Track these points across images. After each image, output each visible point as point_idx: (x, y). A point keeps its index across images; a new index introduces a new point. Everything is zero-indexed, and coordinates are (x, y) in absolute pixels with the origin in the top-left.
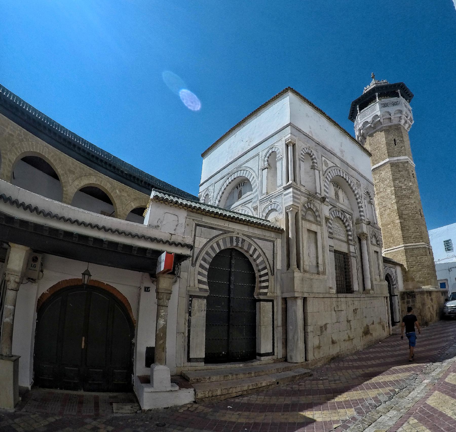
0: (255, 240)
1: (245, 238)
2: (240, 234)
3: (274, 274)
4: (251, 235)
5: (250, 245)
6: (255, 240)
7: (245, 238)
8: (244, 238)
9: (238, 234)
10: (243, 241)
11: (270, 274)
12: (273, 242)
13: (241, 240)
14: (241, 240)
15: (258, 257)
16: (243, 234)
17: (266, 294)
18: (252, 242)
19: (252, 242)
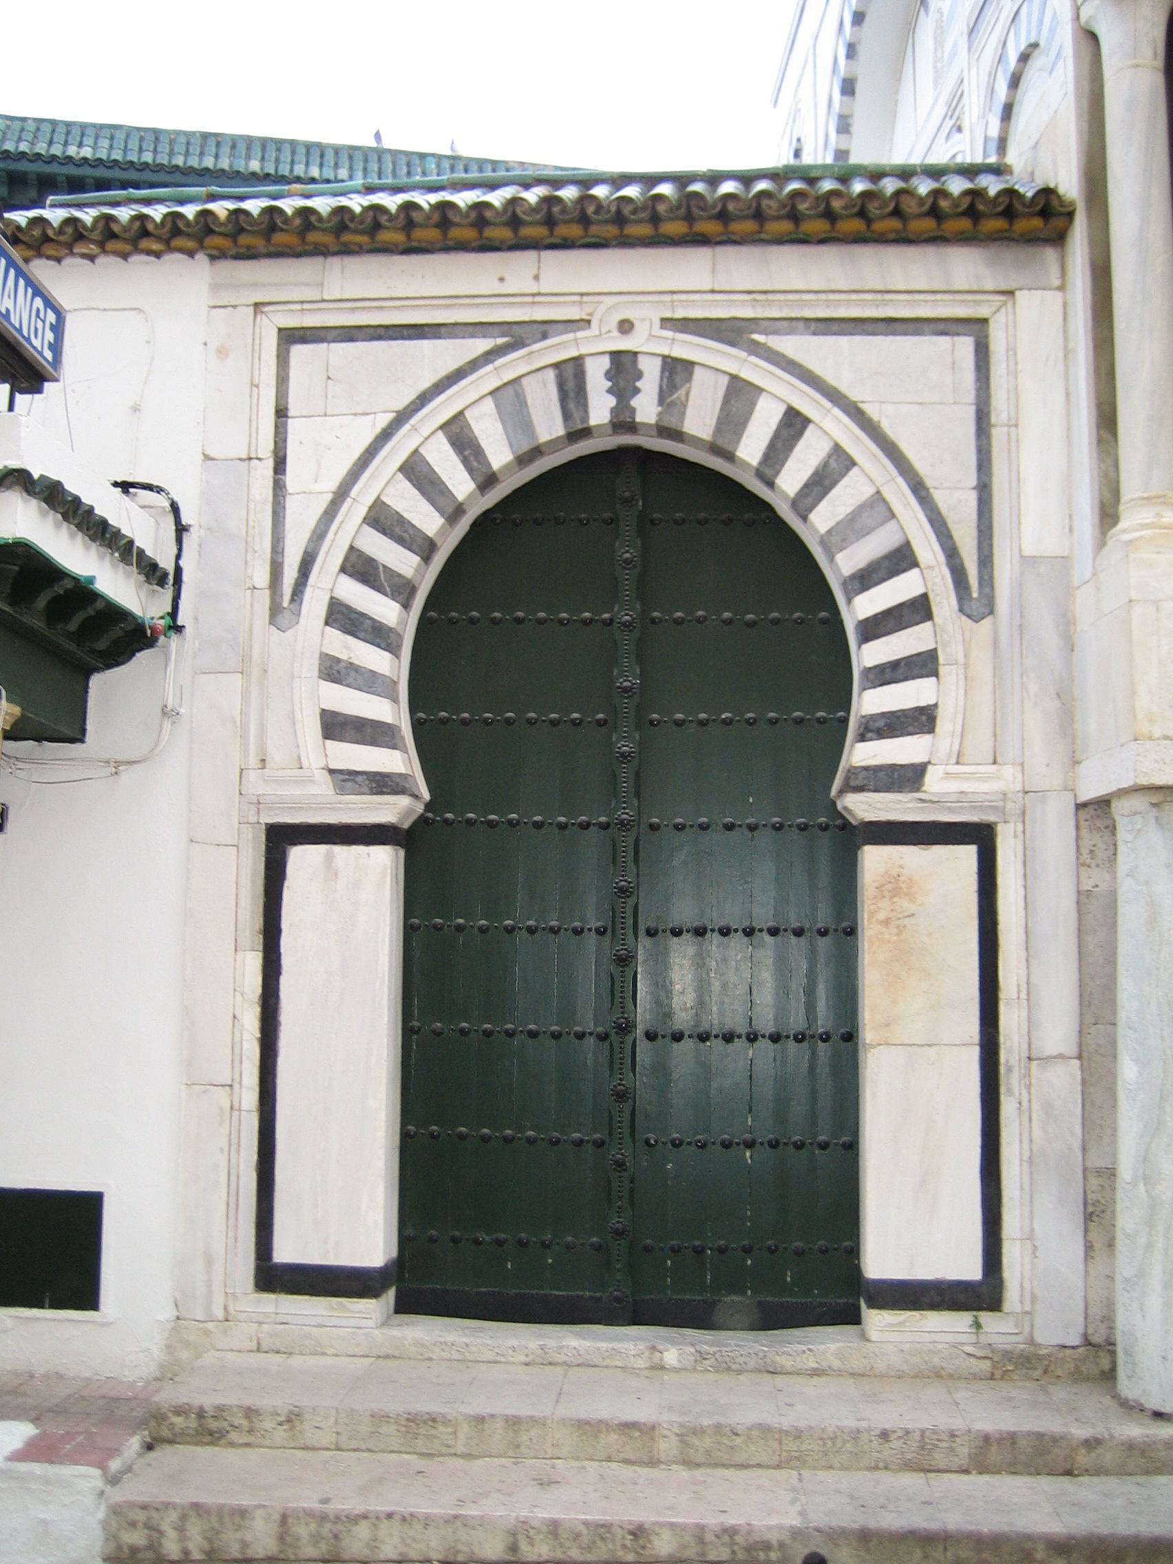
0: (787, 345)
1: (686, 347)
2: (641, 331)
3: (989, 608)
4: (747, 313)
5: (740, 395)
6: (787, 345)
7: (686, 347)
8: (678, 352)
9: (626, 327)
10: (677, 371)
11: (945, 603)
12: (977, 327)
13: (651, 371)
14: (651, 371)
15: (821, 483)
16: (666, 322)
17: (908, 777)
18: (752, 370)
19: (752, 370)
